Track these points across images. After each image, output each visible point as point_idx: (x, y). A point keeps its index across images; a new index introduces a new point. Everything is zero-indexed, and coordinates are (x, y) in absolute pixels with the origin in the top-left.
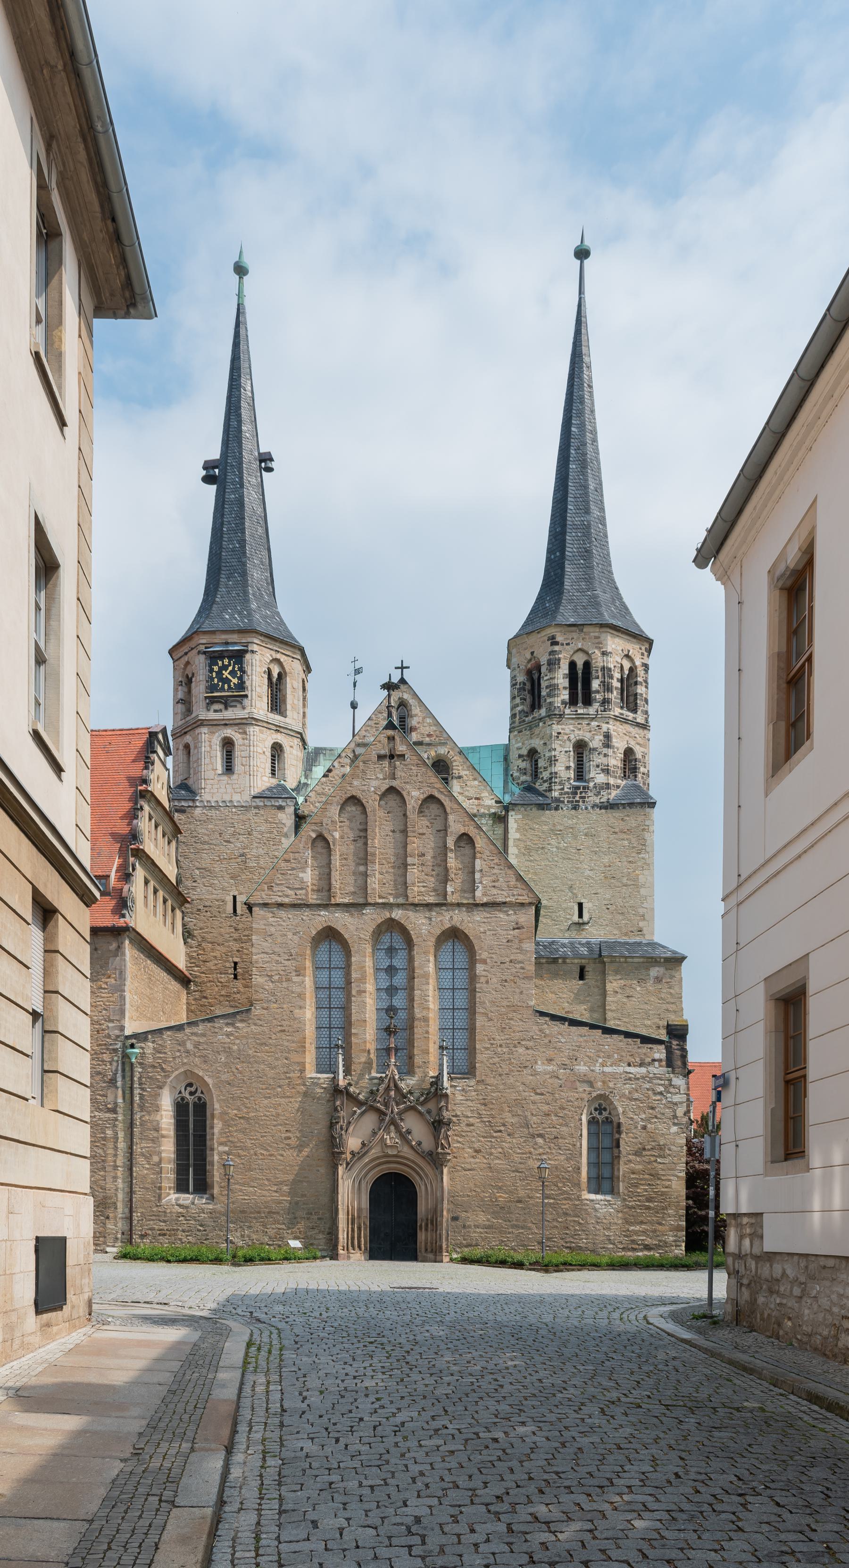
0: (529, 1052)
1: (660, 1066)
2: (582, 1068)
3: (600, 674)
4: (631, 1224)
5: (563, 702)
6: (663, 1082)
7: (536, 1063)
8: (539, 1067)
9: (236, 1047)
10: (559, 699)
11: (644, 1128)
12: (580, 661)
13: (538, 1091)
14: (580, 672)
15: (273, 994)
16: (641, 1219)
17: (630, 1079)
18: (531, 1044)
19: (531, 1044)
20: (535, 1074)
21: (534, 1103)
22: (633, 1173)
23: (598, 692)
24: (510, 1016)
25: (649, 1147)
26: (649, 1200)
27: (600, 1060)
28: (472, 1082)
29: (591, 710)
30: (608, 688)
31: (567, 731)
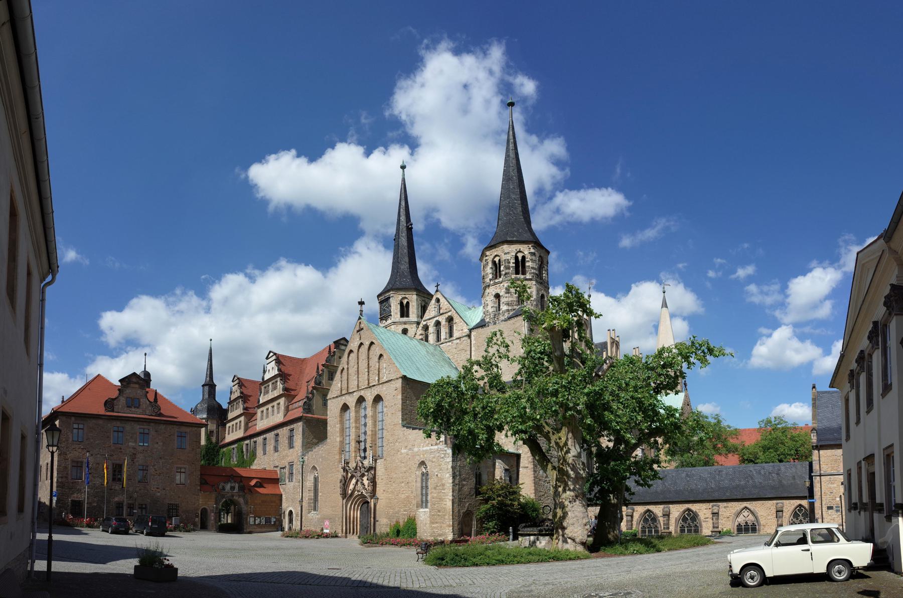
0: (400, 444)
1: (443, 444)
2: (416, 449)
3: (504, 263)
4: (433, 523)
5: (490, 280)
6: (443, 452)
7: (401, 449)
8: (403, 451)
9: (323, 455)
10: (488, 279)
11: (437, 475)
12: (497, 259)
13: (403, 462)
14: (498, 264)
15: (332, 433)
16: (436, 521)
17: (432, 452)
18: (401, 440)
19: (401, 440)
20: (402, 454)
21: (401, 467)
22: (433, 498)
23: (503, 271)
24: (394, 428)
25: (439, 485)
26: (439, 511)
27: (422, 445)
28: (383, 460)
29: (501, 279)
30: (508, 268)
31: (492, 291)
